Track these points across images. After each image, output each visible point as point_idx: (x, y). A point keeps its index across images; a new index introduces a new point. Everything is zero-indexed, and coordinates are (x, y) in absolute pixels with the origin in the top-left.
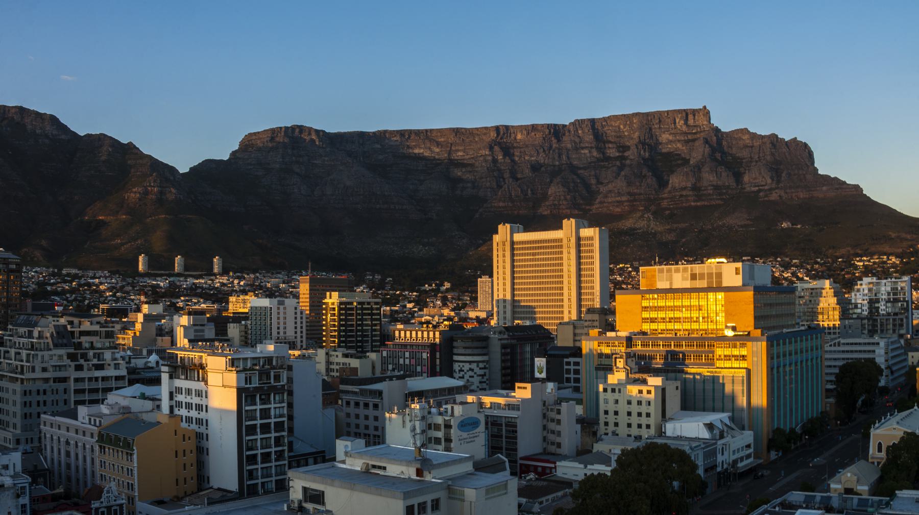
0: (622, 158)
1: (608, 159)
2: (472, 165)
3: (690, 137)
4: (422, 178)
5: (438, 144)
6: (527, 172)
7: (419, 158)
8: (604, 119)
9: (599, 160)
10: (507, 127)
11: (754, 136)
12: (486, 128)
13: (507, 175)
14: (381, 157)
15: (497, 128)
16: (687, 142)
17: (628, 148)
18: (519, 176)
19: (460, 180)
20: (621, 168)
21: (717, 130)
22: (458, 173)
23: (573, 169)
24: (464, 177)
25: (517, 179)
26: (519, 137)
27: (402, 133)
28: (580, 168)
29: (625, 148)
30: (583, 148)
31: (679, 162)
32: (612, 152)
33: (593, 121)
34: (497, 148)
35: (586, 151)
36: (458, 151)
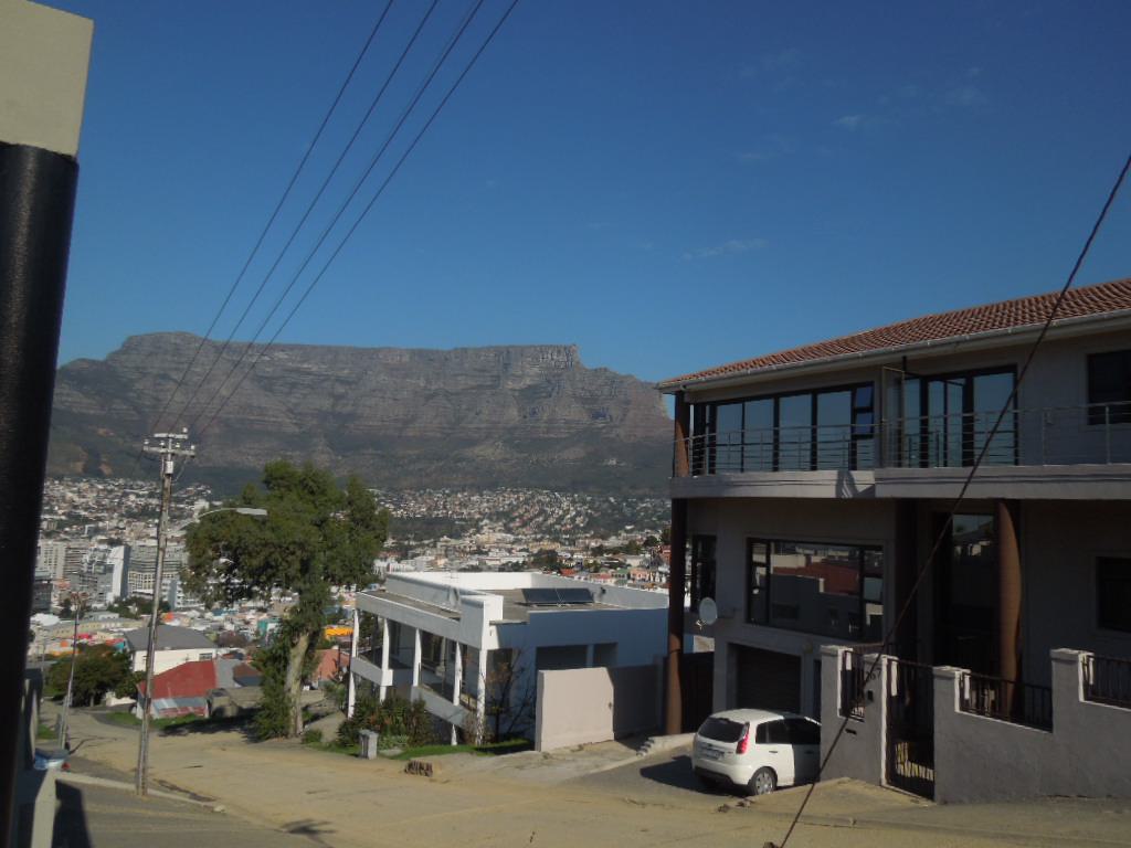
4: (304, 392)
18: (398, 397)
22: (340, 389)
25: (395, 400)
28: (452, 394)
30: (458, 375)
31: (544, 395)
35: (459, 378)
36: (344, 369)
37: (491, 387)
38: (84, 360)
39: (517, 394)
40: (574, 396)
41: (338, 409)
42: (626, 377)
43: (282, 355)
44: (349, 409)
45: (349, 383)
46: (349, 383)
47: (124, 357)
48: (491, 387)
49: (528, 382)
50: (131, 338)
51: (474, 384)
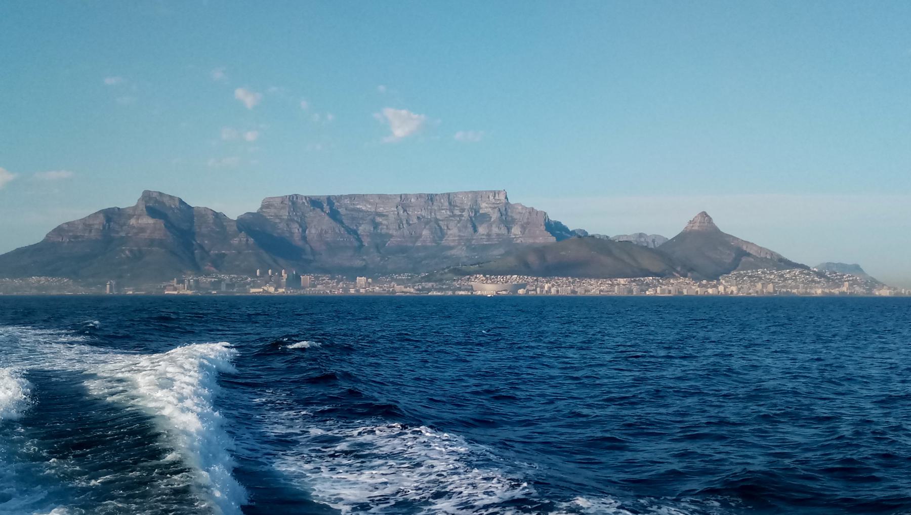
0: (461, 216)
1: (454, 216)
2: (387, 216)
5: (370, 203)
6: (415, 221)
7: (360, 210)
8: (456, 194)
9: (450, 216)
13: (404, 222)
19: (381, 224)
20: (459, 222)
22: (379, 219)
23: (437, 221)
24: (385, 222)
29: (463, 210)
32: (457, 212)
33: (449, 194)
34: (400, 207)
44: (384, 231)
46: (384, 216)
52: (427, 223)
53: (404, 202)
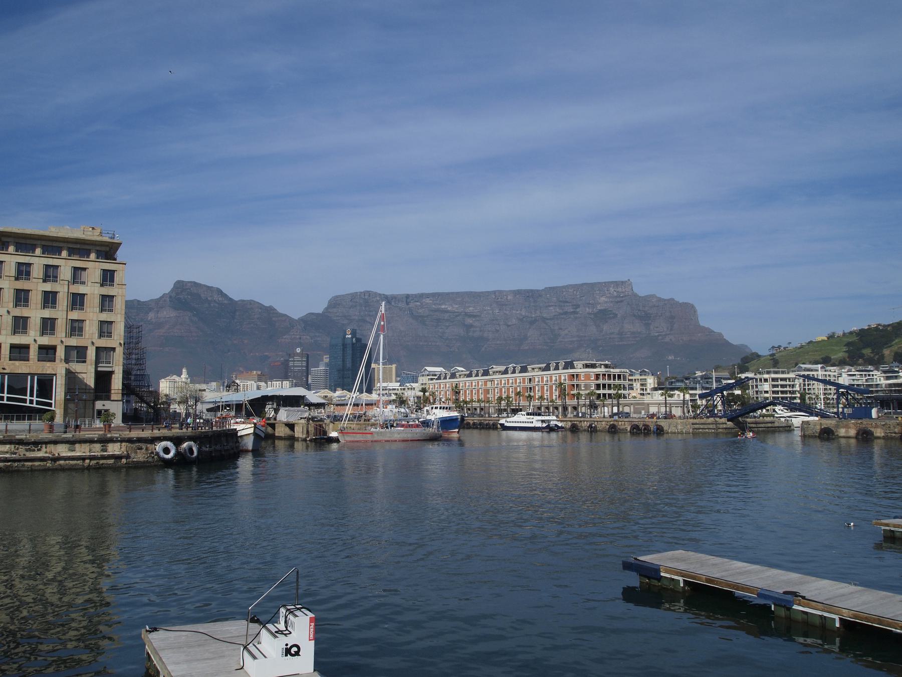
1: (566, 313)
3: (619, 299)
8: (563, 287)
10: (500, 292)
11: (660, 300)
12: (488, 292)
14: (420, 311)
15: (494, 292)
16: (618, 302)
17: (578, 306)
19: (471, 326)
21: (635, 295)
22: (469, 321)
23: (544, 320)
25: (508, 326)
26: (509, 298)
27: (433, 295)
37: (574, 313)
38: (313, 314)
39: (592, 316)
40: (635, 316)
41: (470, 334)
42: (669, 300)
43: (428, 301)
45: (475, 316)
46: (475, 316)
47: (335, 310)
48: (574, 313)
49: (599, 307)
50: (337, 297)
51: (561, 311)
52: (532, 322)
53: (497, 298)
